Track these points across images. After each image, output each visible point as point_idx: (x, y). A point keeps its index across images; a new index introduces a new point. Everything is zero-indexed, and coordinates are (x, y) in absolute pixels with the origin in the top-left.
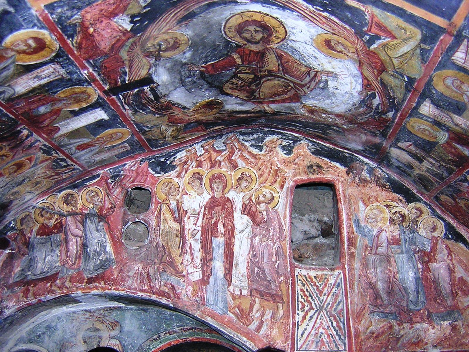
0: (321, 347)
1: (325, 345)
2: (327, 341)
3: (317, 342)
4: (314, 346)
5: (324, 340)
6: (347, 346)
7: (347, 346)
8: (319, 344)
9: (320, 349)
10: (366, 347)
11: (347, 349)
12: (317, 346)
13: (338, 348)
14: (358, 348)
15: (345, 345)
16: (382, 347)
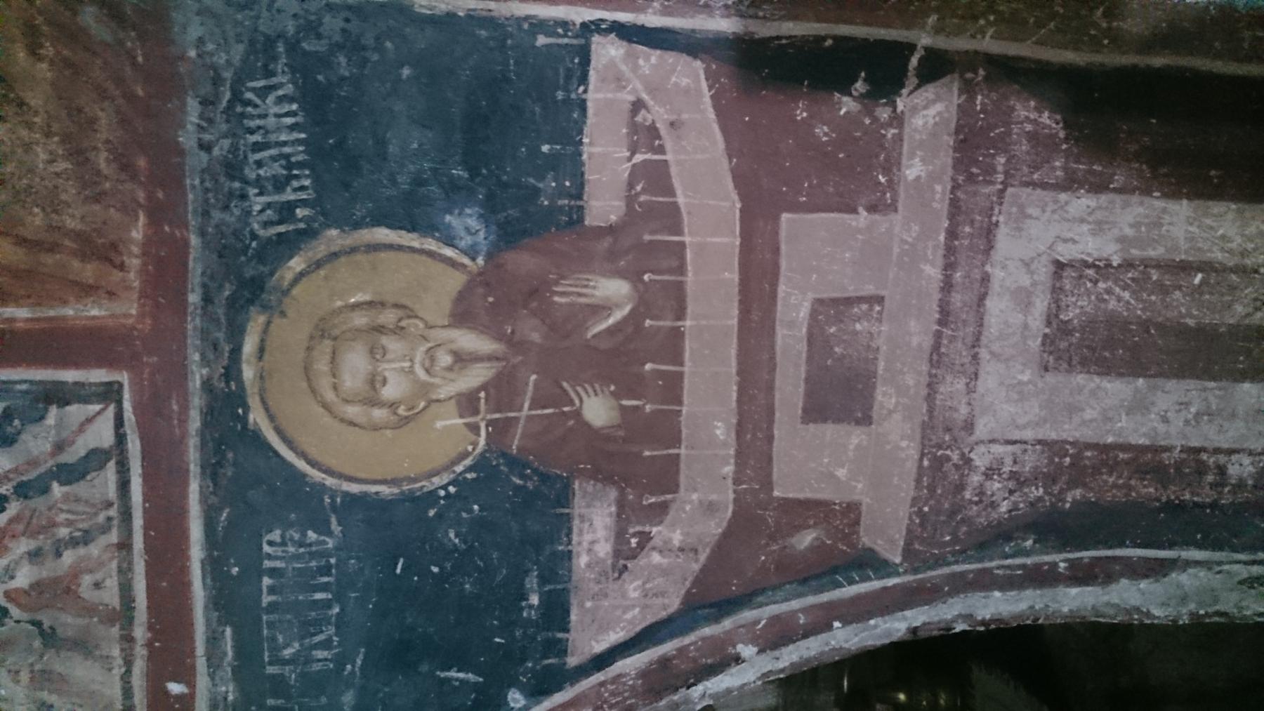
0: (90, 610)
1: (75, 574)
2: (35, 556)
3: (50, 638)
4: (80, 670)
5: (23, 578)
6: (70, 376)
7: (70, 376)
8: (68, 622)
9: (110, 618)
10: (70, 192)
11: (98, 376)
12: (83, 646)
13: (96, 459)
14: (88, 271)
15: (58, 395)
16: (73, 35)
